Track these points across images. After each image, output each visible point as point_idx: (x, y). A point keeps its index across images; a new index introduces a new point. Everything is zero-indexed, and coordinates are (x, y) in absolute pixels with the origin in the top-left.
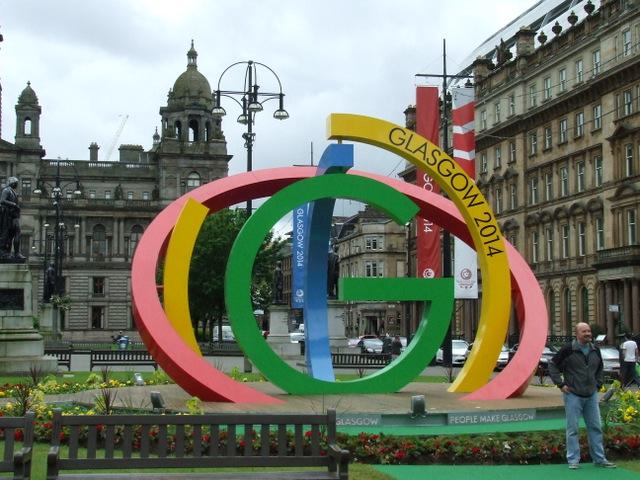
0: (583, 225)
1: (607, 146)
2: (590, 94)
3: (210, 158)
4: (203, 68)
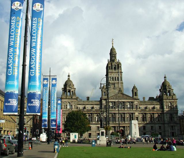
3: (173, 99)
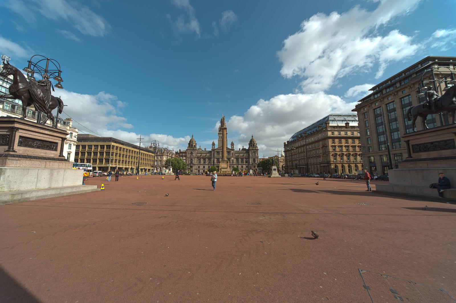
0: (317, 158)
1: (321, 149)
2: (318, 141)
3: (256, 150)
4: (254, 138)
